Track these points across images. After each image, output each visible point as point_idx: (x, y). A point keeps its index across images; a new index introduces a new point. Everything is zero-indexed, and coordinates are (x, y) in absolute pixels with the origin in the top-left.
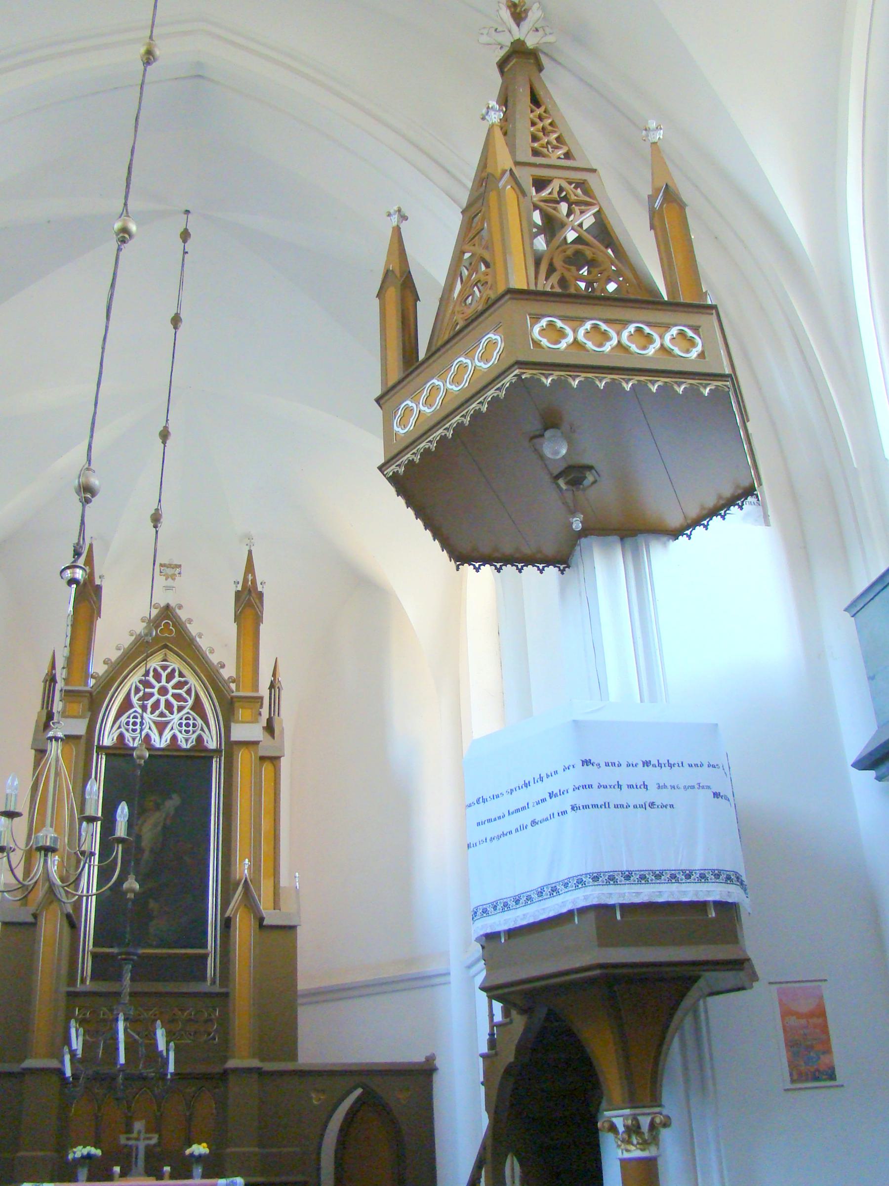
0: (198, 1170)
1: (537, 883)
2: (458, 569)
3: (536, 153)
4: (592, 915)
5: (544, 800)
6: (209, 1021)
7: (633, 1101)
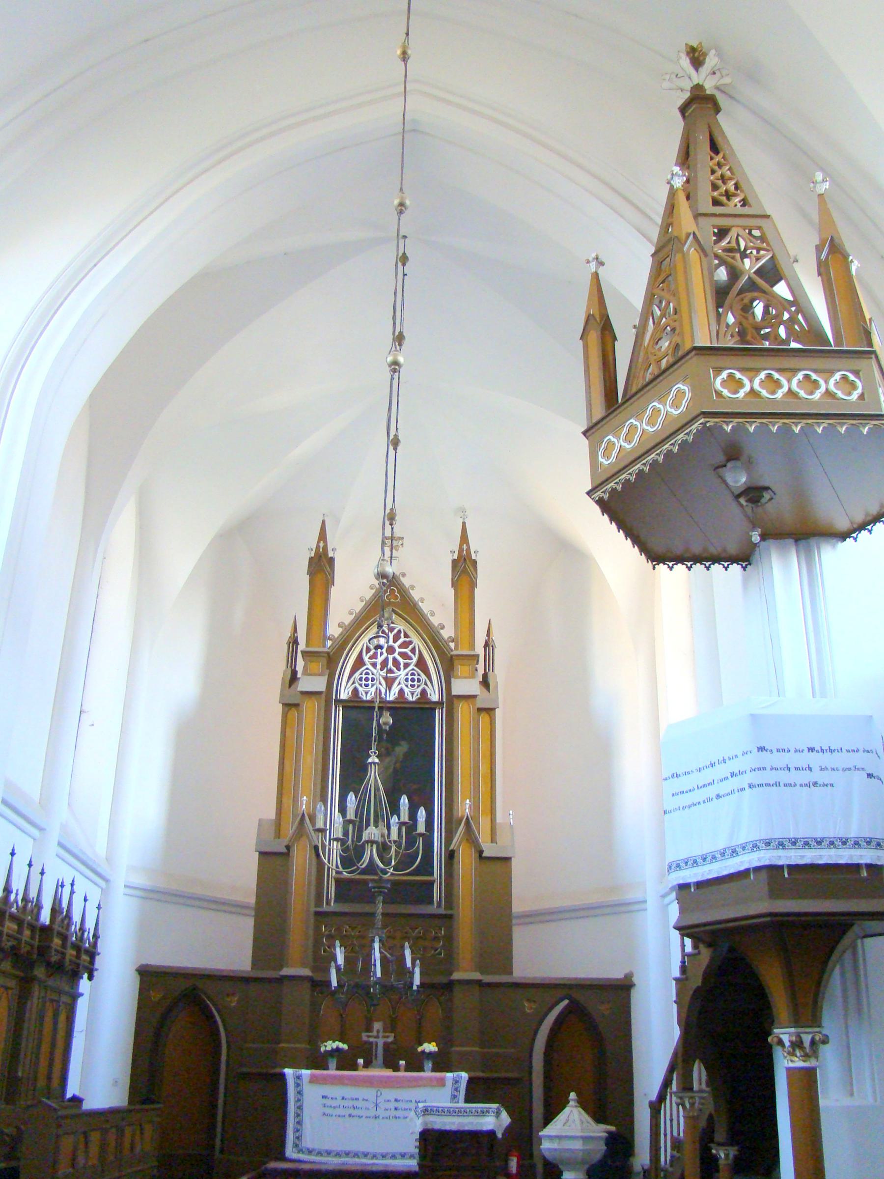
0: (429, 1065)
1: (721, 845)
2: (654, 568)
3: (716, 202)
4: (764, 875)
5: (726, 778)
6: (436, 938)
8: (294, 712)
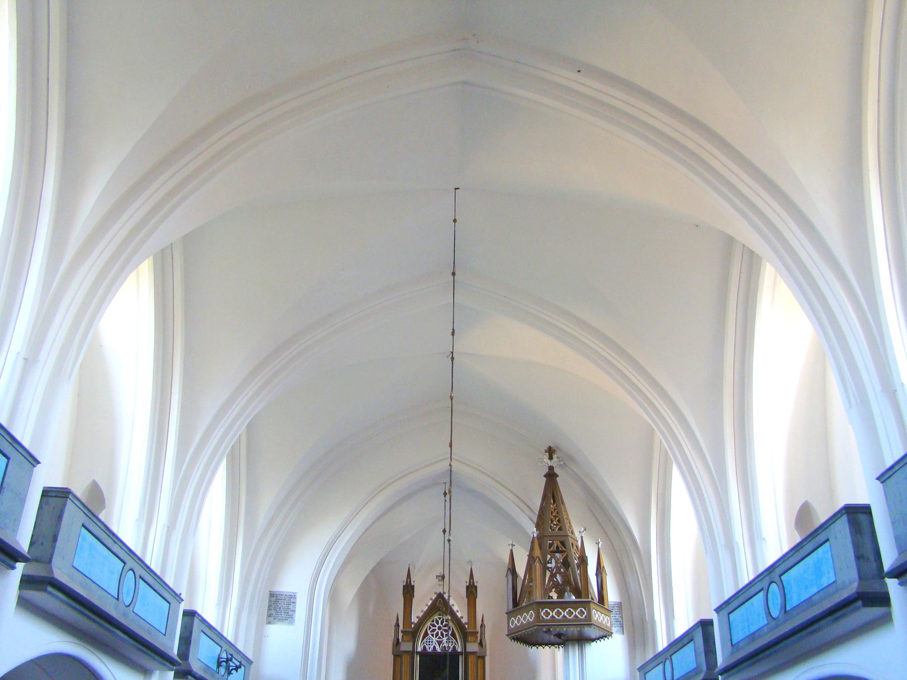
8: (399, 659)
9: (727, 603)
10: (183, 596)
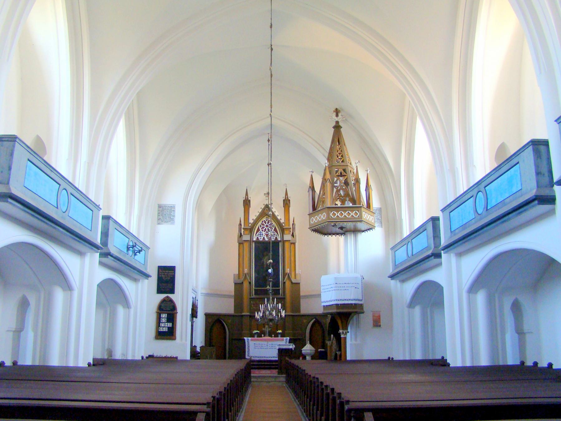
0: (280, 336)
7: (343, 329)
8: (241, 245)
9: (449, 205)
10: (101, 207)
